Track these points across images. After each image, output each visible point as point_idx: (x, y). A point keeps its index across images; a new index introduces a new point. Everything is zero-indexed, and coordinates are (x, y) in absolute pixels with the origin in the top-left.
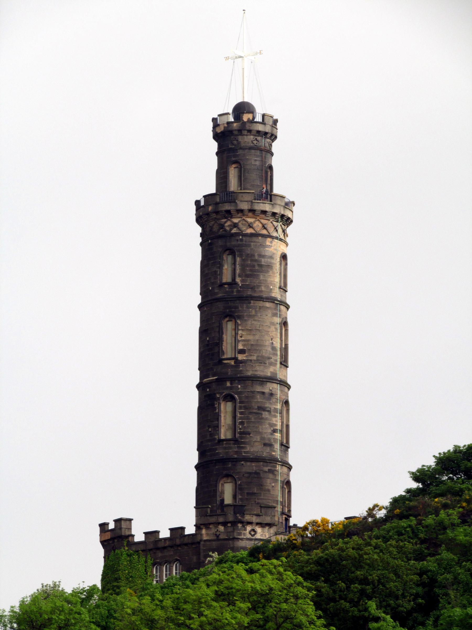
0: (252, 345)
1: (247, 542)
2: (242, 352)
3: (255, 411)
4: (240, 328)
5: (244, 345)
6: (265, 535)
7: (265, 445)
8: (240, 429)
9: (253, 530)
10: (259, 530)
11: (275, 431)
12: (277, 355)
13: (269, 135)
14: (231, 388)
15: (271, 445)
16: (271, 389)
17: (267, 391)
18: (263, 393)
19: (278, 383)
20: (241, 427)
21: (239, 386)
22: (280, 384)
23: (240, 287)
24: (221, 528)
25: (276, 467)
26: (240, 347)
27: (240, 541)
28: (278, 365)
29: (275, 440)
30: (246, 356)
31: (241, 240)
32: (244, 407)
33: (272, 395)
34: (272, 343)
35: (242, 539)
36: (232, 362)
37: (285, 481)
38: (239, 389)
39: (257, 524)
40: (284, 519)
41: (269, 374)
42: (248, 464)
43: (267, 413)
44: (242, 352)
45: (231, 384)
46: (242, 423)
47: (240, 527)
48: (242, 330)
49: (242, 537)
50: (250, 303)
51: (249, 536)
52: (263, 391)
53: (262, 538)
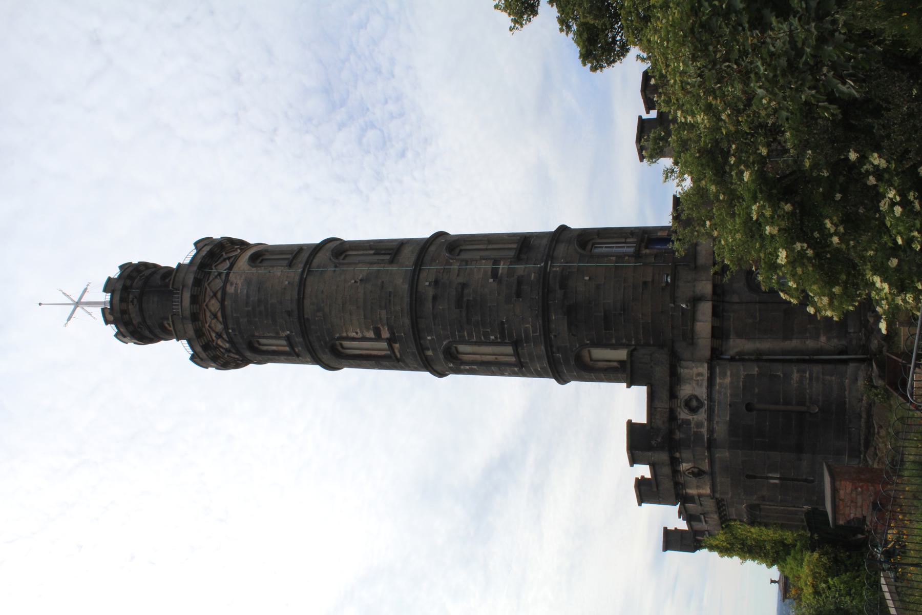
0: (365, 317)
1: (716, 419)
2: (377, 332)
3: (464, 314)
4: (344, 335)
5: (368, 329)
6: (699, 374)
7: (519, 294)
8: (496, 338)
9: (687, 403)
10: (686, 390)
11: (495, 274)
12: (378, 270)
13: (129, 283)
14: (434, 350)
15: (520, 282)
16: (427, 284)
17: (431, 292)
18: (435, 298)
19: (420, 269)
20: (492, 337)
21: (429, 338)
22: (421, 266)
23: (291, 332)
24: (684, 466)
25: (556, 271)
26: (371, 334)
27: (715, 436)
28: (394, 268)
29: (511, 272)
30: (383, 326)
31: (233, 330)
32: (459, 332)
33: (436, 282)
34: (361, 280)
35: (711, 431)
36: (397, 346)
37: (580, 250)
38: (433, 339)
39: (673, 395)
40: (648, 251)
41: (406, 286)
42: (553, 326)
43: (466, 291)
44: (377, 332)
45: (428, 349)
46: (486, 335)
47: (682, 436)
48: (347, 331)
49: (704, 430)
50: (308, 319)
51: (702, 416)
52: (430, 298)
53: (705, 383)
